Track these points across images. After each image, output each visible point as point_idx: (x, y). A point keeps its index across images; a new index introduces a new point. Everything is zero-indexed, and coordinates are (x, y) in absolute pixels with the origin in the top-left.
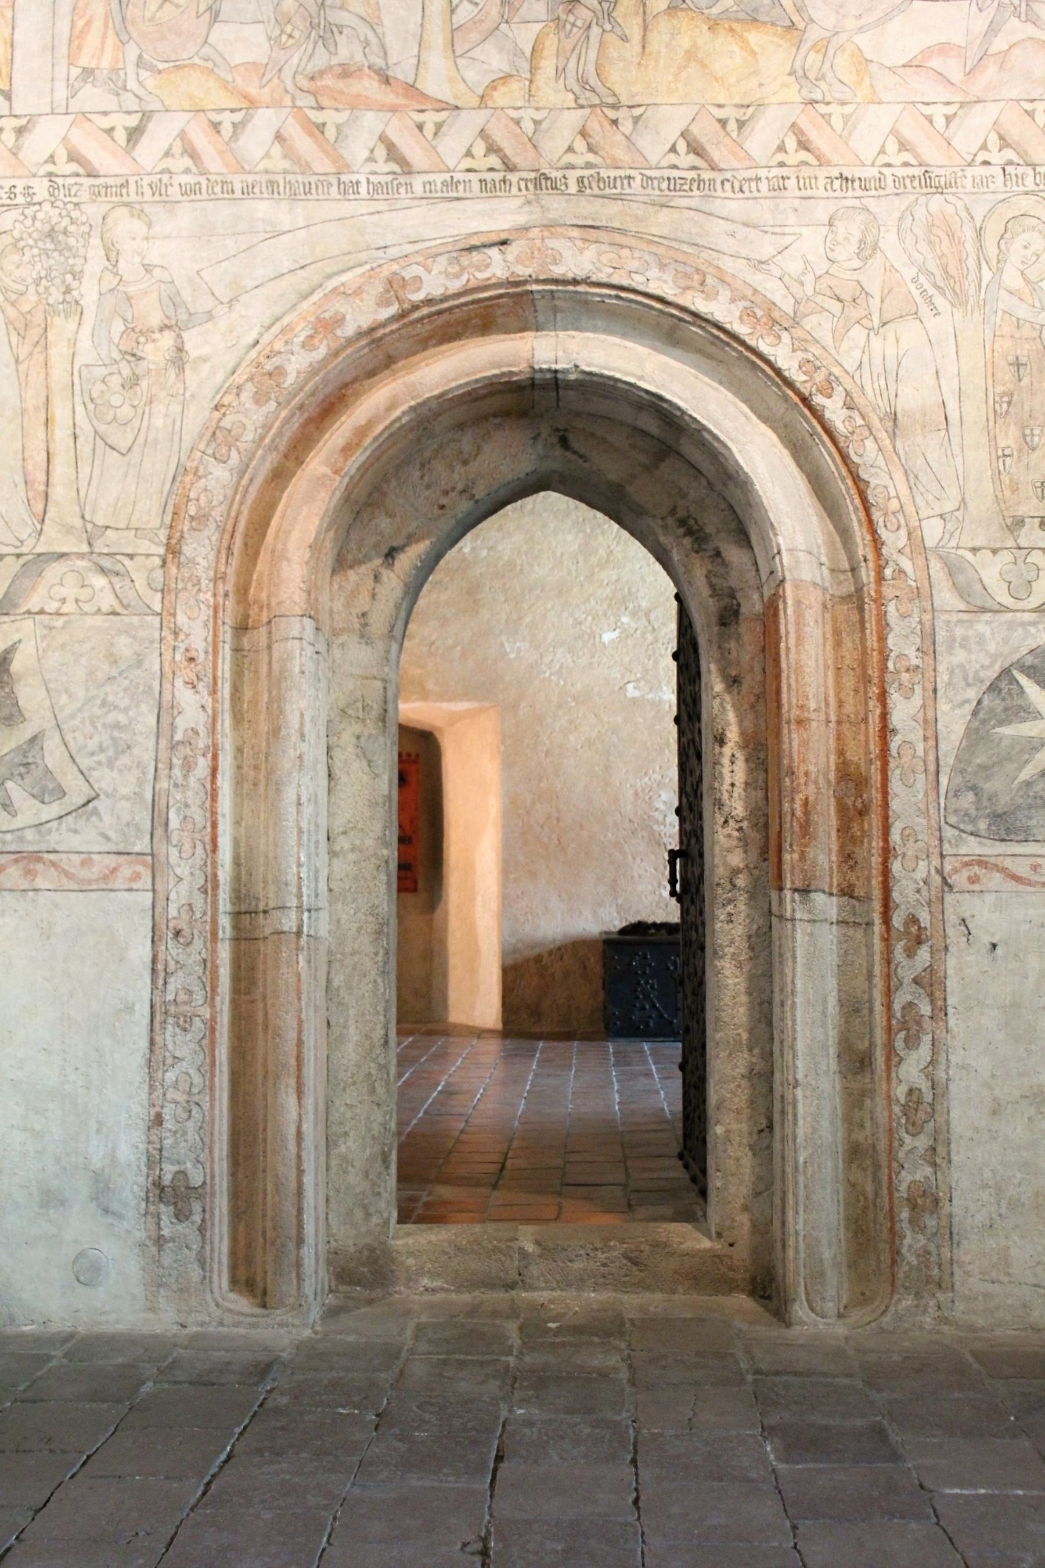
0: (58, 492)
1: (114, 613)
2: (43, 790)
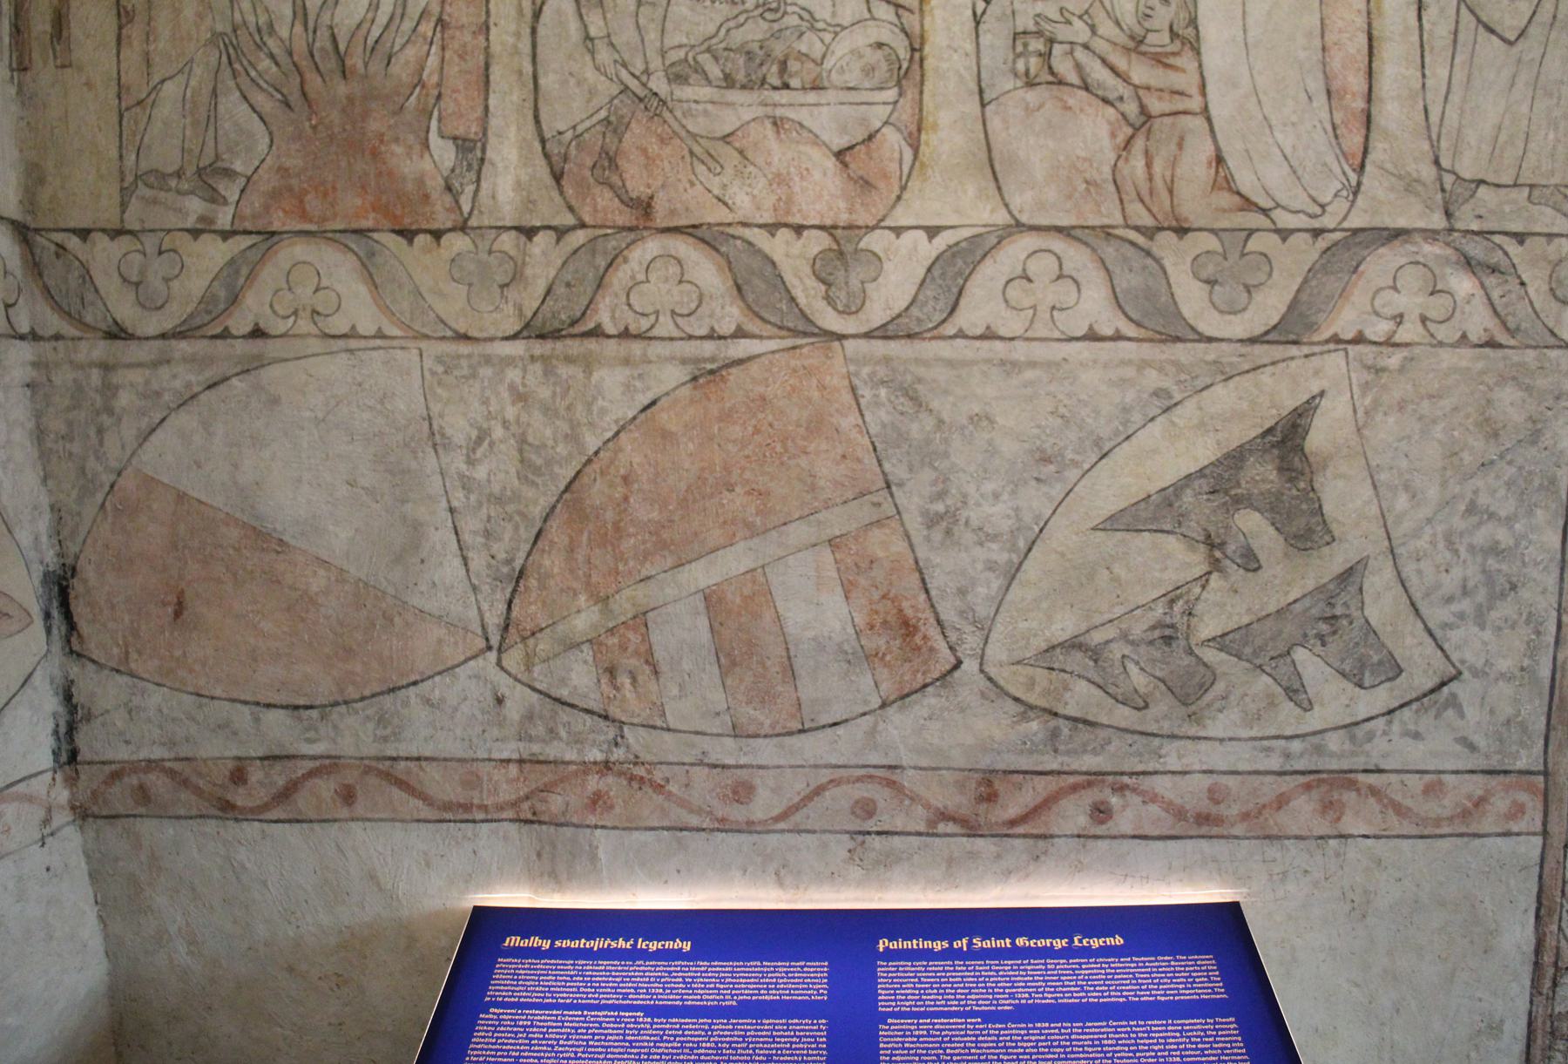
0: (1393, 112)
1: (1492, 344)
2: (1362, 664)
